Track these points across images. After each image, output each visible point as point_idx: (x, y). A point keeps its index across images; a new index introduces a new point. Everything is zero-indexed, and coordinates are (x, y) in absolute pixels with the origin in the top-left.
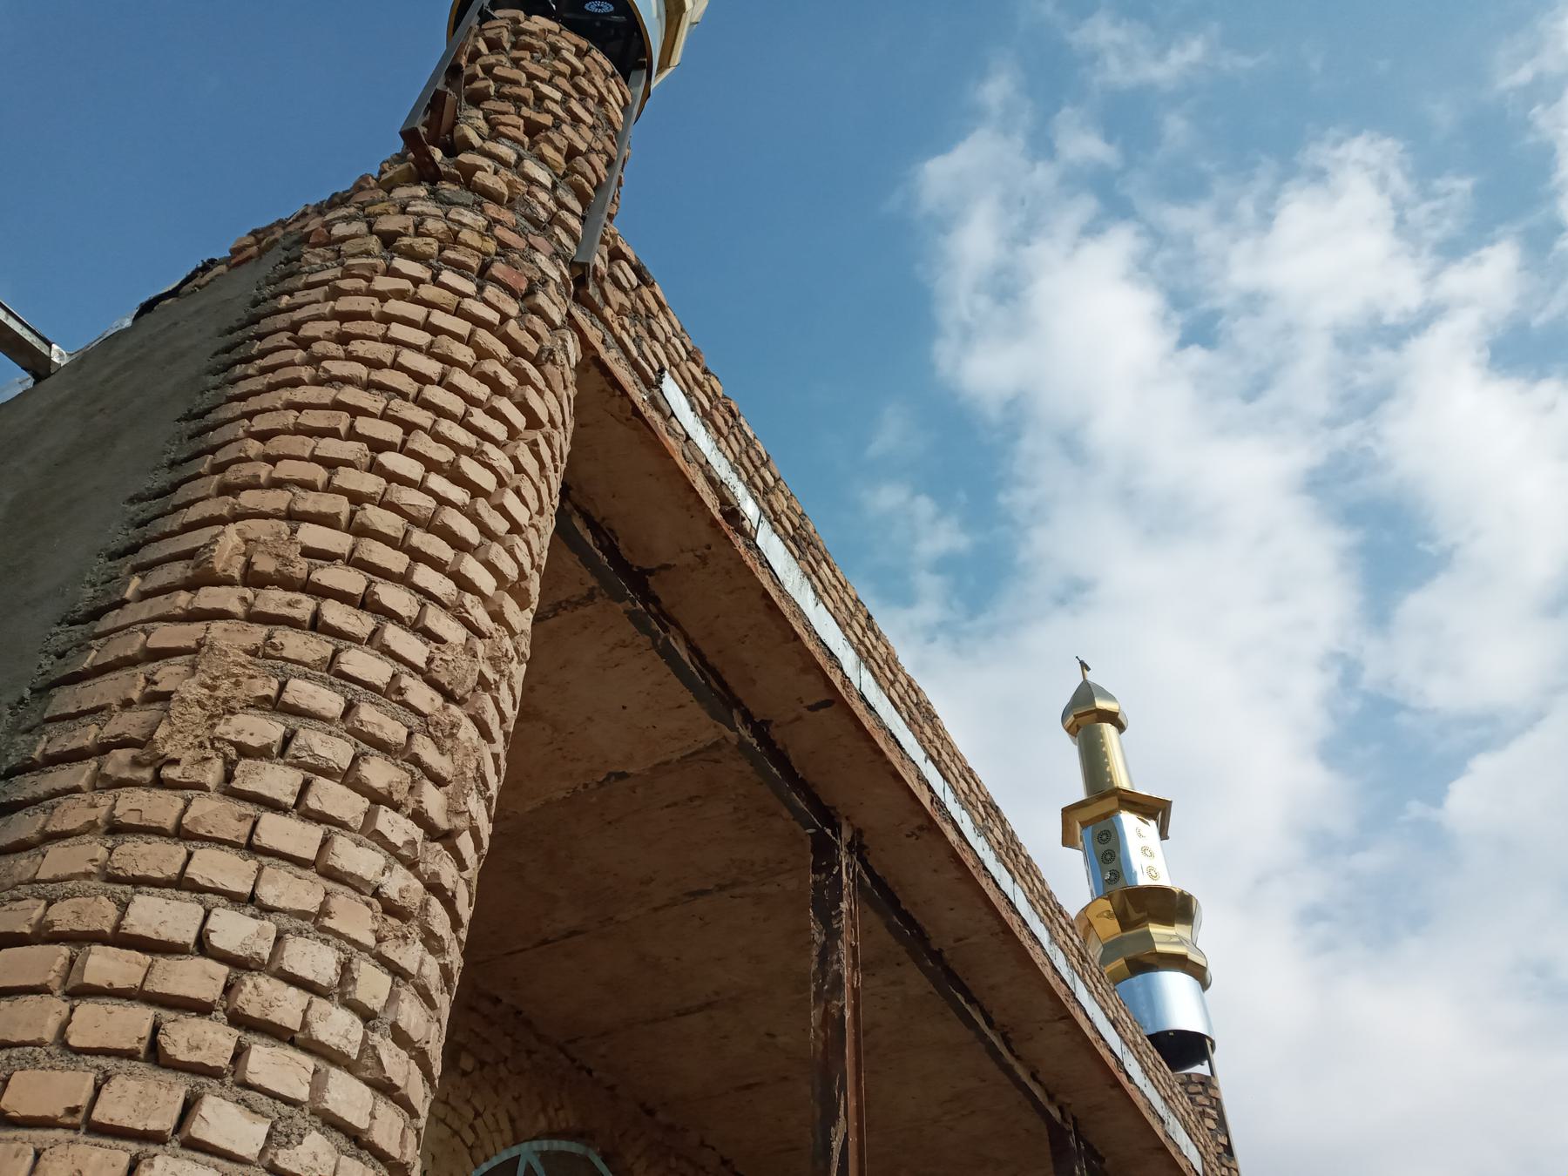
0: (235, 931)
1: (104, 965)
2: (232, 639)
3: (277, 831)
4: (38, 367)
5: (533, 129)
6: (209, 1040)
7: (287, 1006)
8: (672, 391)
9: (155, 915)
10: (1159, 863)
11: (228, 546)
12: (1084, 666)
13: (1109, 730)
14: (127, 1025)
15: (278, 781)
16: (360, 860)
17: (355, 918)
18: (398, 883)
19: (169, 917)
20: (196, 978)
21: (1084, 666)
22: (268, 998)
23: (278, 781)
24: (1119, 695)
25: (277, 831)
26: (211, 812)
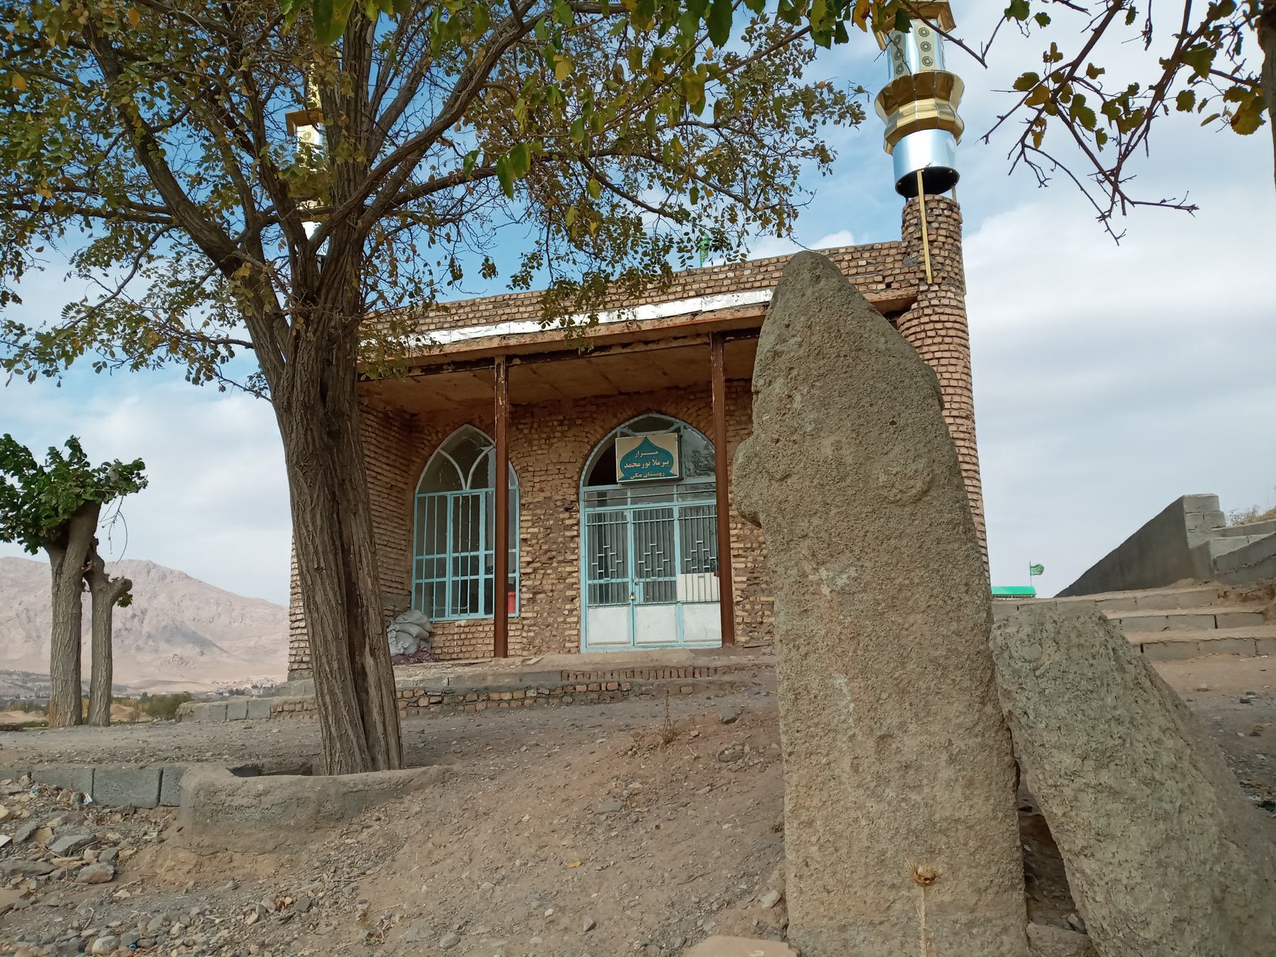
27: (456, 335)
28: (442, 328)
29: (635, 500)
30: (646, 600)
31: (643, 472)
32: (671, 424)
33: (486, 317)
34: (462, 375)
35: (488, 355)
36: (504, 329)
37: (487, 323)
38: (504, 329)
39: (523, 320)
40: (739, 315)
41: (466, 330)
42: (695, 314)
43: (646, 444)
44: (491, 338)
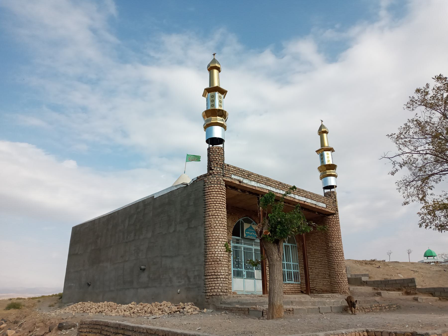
0: (217, 235)
1: (213, 237)
2: (212, 220)
3: (218, 230)
4: (187, 185)
5: (217, 163)
6: (218, 239)
7: (220, 237)
8: (233, 176)
9: (214, 235)
10: (330, 159)
11: (210, 213)
12: (322, 121)
13: (325, 135)
14: (215, 239)
15: (216, 227)
16: (221, 230)
17: (222, 232)
18: (223, 230)
19: (214, 235)
20: (217, 237)
21: (322, 121)
22: (219, 237)
23: (216, 227)
24: (328, 126)
25: (218, 230)
26: (215, 230)
27: (258, 185)
28: (255, 181)
29: (245, 244)
30: (247, 277)
31: (250, 235)
32: (252, 222)
33: (265, 183)
34: (251, 196)
35: (258, 193)
36: (269, 188)
37: (265, 185)
38: (269, 188)
39: (274, 188)
40: (312, 205)
41: (261, 184)
42: (304, 202)
43: (251, 227)
44: (266, 189)
